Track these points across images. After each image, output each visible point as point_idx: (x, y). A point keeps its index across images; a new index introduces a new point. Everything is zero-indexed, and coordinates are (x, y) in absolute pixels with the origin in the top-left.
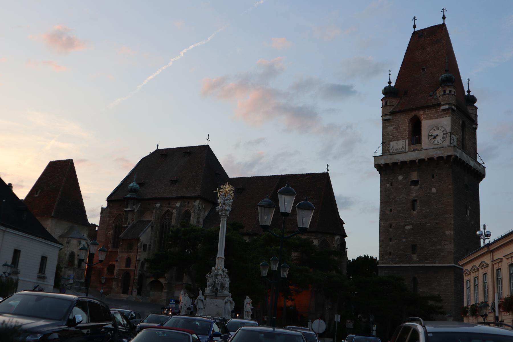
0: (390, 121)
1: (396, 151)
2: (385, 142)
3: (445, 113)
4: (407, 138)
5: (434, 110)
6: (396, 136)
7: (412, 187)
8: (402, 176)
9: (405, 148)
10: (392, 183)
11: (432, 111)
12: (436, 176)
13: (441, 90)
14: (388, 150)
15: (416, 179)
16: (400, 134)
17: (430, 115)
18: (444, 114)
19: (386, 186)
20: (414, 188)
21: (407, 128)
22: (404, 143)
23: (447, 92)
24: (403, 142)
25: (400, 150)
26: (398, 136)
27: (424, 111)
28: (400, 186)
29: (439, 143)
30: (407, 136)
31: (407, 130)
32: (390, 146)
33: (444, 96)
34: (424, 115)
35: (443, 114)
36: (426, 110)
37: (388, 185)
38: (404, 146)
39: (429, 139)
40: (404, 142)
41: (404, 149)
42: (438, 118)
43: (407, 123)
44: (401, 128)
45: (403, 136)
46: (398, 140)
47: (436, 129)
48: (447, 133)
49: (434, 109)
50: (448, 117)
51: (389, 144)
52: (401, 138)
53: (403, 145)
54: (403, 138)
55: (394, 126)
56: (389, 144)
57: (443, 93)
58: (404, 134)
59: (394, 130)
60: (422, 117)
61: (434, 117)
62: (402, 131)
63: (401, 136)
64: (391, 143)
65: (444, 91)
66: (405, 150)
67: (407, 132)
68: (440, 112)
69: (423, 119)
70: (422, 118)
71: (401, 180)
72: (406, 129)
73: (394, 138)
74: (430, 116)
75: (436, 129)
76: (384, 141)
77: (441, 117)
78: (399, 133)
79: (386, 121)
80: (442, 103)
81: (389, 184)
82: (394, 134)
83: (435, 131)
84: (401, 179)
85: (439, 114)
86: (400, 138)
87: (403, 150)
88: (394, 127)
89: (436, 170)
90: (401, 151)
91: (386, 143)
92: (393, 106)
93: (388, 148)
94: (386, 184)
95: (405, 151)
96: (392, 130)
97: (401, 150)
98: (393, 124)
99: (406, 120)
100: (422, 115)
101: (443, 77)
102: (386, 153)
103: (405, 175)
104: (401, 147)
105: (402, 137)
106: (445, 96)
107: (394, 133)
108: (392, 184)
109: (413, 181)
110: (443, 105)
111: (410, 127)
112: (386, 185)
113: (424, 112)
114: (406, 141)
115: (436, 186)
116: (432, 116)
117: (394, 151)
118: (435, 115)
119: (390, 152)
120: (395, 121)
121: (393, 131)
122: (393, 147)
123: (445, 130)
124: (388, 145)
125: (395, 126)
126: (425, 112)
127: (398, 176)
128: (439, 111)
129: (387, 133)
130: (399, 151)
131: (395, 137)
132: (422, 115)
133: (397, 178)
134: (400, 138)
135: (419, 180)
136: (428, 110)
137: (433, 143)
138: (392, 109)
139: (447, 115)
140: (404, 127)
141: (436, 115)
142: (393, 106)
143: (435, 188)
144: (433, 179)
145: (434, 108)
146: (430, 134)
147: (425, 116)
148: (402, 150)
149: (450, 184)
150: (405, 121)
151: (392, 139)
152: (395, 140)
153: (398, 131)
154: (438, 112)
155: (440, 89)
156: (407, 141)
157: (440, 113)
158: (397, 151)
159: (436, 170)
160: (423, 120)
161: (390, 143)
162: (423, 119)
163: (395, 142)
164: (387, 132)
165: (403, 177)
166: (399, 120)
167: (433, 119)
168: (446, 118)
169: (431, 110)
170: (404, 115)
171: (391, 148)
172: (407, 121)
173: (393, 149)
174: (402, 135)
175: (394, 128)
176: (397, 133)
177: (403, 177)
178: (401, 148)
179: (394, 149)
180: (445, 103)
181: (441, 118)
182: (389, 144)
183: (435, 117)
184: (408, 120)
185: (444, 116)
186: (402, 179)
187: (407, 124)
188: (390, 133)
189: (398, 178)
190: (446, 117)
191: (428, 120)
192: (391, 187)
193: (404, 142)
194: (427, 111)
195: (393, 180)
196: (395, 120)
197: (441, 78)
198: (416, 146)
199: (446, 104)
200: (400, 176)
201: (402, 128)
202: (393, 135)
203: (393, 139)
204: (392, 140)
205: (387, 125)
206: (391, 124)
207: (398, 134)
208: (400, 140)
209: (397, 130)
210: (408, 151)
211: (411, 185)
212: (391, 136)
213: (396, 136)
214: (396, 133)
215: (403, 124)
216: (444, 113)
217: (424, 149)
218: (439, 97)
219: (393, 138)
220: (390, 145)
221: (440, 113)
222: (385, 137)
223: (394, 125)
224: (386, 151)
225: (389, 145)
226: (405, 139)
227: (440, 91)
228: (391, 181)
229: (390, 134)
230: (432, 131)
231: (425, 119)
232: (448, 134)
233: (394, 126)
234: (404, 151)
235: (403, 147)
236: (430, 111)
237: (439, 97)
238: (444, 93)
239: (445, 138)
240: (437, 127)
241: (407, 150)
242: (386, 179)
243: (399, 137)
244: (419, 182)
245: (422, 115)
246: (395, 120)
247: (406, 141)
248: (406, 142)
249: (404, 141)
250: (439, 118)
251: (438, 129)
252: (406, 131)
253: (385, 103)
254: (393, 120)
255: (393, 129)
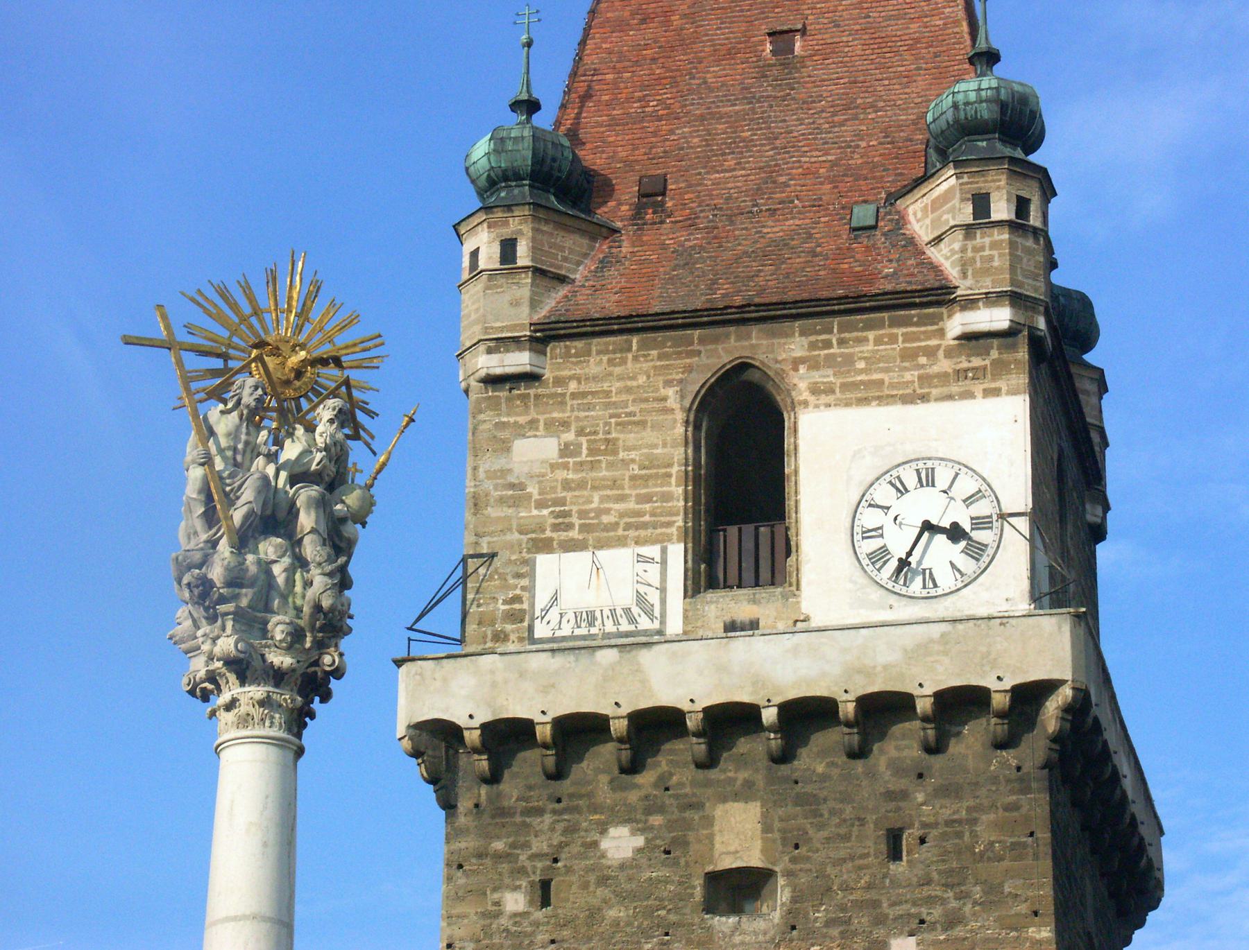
0: (532, 392)
1: (583, 631)
2: (493, 556)
3: (987, 362)
4: (673, 530)
5: (893, 339)
6: (583, 514)
7: (723, 923)
8: (633, 833)
9: (657, 613)
10: (545, 886)
11: (878, 341)
12: (922, 841)
13: (951, 190)
14: (515, 617)
15: (754, 859)
16: (622, 498)
17: (861, 371)
18: (979, 373)
19: (497, 904)
20: (736, 928)
21: (679, 453)
22: (653, 573)
23: (1001, 210)
24: (641, 559)
25: (616, 623)
26: (600, 512)
27: (813, 338)
28: (612, 913)
29: (935, 586)
30: (679, 521)
31: (675, 470)
32: (531, 589)
33: (981, 239)
34: (814, 365)
35: (966, 370)
36: (831, 332)
37: (515, 902)
38: (654, 597)
39: (855, 553)
40: (651, 560)
41: (650, 615)
42: (924, 398)
43: (680, 416)
44: (622, 455)
45: (639, 514)
46: (601, 547)
47: (910, 480)
48: (1002, 516)
49: (900, 331)
50: (1013, 392)
51: (527, 571)
52: (628, 527)
53: (642, 589)
54: (642, 533)
55: (570, 436)
56: (524, 570)
57: (966, 213)
58: (647, 499)
59: (565, 466)
60: (801, 382)
61: (892, 386)
62: (633, 478)
63: (622, 515)
64: (544, 562)
65: (981, 204)
66: (663, 622)
67: (680, 490)
68: (941, 353)
69: (806, 395)
70: (802, 385)
71: (622, 867)
72: (670, 465)
73: (569, 527)
74: (863, 377)
75: (910, 480)
76: (485, 550)
77: (955, 389)
78: (609, 492)
79: (503, 394)
80: (964, 288)
81: (516, 888)
82: (569, 495)
83: (902, 490)
84: (630, 854)
85: (936, 369)
86: (620, 532)
87: (645, 623)
88: (567, 445)
89: (920, 797)
90: (627, 634)
91: (497, 562)
92: (562, 279)
93: (517, 599)
94: (495, 890)
95: (660, 632)
96: (553, 467)
97: (625, 627)
98: (555, 415)
99: (670, 392)
100: (802, 370)
101: (972, 96)
102: (501, 637)
103: (656, 820)
104: (625, 597)
105: (638, 527)
106: (987, 240)
107: (567, 486)
108: (544, 893)
109: (715, 880)
110: (969, 303)
111: (697, 449)
112: (496, 896)
113: (813, 346)
114: (664, 551)
115: (922, 922)
116: (881, 382)
117: (566, 631)
118: (908, 376)
119: (533, 641)
120: (574, 396)
121: (561, 474)
122: (555, 599)
123: (985, 491)
124: (518, 576)
125: (580, 432)
126: (828, 345)
127: (603, 832)
128: (939, 346)
129: (512, 486)
130: (610, 627)
131: (575, 520)
132: (796, 362)
133: (595, 844)
134: (620, 532)
135: (777, 869)
136: (847, 335)
137: (890, 585)
138: (552, 302)
139: (1002, 384)
140: (655, 446)
141: (916, 373)
142: (562, 279)
143: (913, 940)
144: (893, 867)
145: (895, 323)
146: (870, 518)
147: (826, 376)
148: (632, 620)
149: (1036, 913)
150: (665, 399)
151: (548, 534)
152: (570, 546)
153: (604, 473)
154: (931, 353)
155: (947, 181)
156: (677, 553)
157: (944, 365)
158: (594, 631)
159: (920, 797)
160: (805, 404)
161: (531, 564)
162: (806, 395)
163: (579, 561)
164: (512, 479)
165: (640, 841)
166: (607, 394)
167: (884, 400)
168: (992, 402)
169: (871, 335)
170: (654, 353)
171: (541, 600)
172: (673, 402)
173: (553, 615)
174: (631, 505)
175: (566, 450)
176: (594, 488)
177: (640, 841)
178: (627, 611)
179: (571, 616)
180: (987, 285)
181: (950, 397)
182: (524, 570)
183: (909, 391)
184: (682, 397)
185: (978, 388)
186: (639, 850)
187: (680, 429)
188: (533, 489)
189: (605, 844)
190: (996, 392)
191: (848, 404)
192: (539, 915)
193: (651, 560)
194: (842, 342)
195: (556, 860)
196: (573, 386)
197: (955, 106)
198: (754, 601)
199: (992, 299)
200: (613, 831)
201: (633, 455)
202: (562, 502)
203: (563, 535)
204: (551, 540)
205: (505, 419)
206: (542, 418)
207: (602, 499)
208: (621, 542)
209: (593, 466)
210: (687, 636)
211: (710, 907)
212: (545, 512)
213: (583, 514)
214: (581, 485)
215: (642, 424)
216: (977, 362)
217: (814, 624)
218: (938, 240)
219: (556, 528)
220: (532, 575)
221: (944, 365)
222: (493, 512)
223: (565, 424)
224: (498, 627)
225: (525, 582)
226: (662, 540)
227: (946, 197)
228: (539, 865)
229: (536, 496)
230: (883, 493)
231: (824, 399)
232: (1012, 520)
233: (570, 436)
234: (645, 633)
235: (641, 599)
236: (866, 340)
237: (938, 240)
238: (976, 215)
239: (990, 551)
240: (921, 465)
241: (675, 626)
242: (499, 845)
243: (606, 519)
244: (781, 881)
245: (796, 369)
246: (573, 386)
247: (664, 551)
248: (664, 562)
249: (653, 551)
250: (936, 400)
251: (927, 480)
252: (670, 476)
253: (496, 249)
254: (559, 390)
255: (561, 457)
